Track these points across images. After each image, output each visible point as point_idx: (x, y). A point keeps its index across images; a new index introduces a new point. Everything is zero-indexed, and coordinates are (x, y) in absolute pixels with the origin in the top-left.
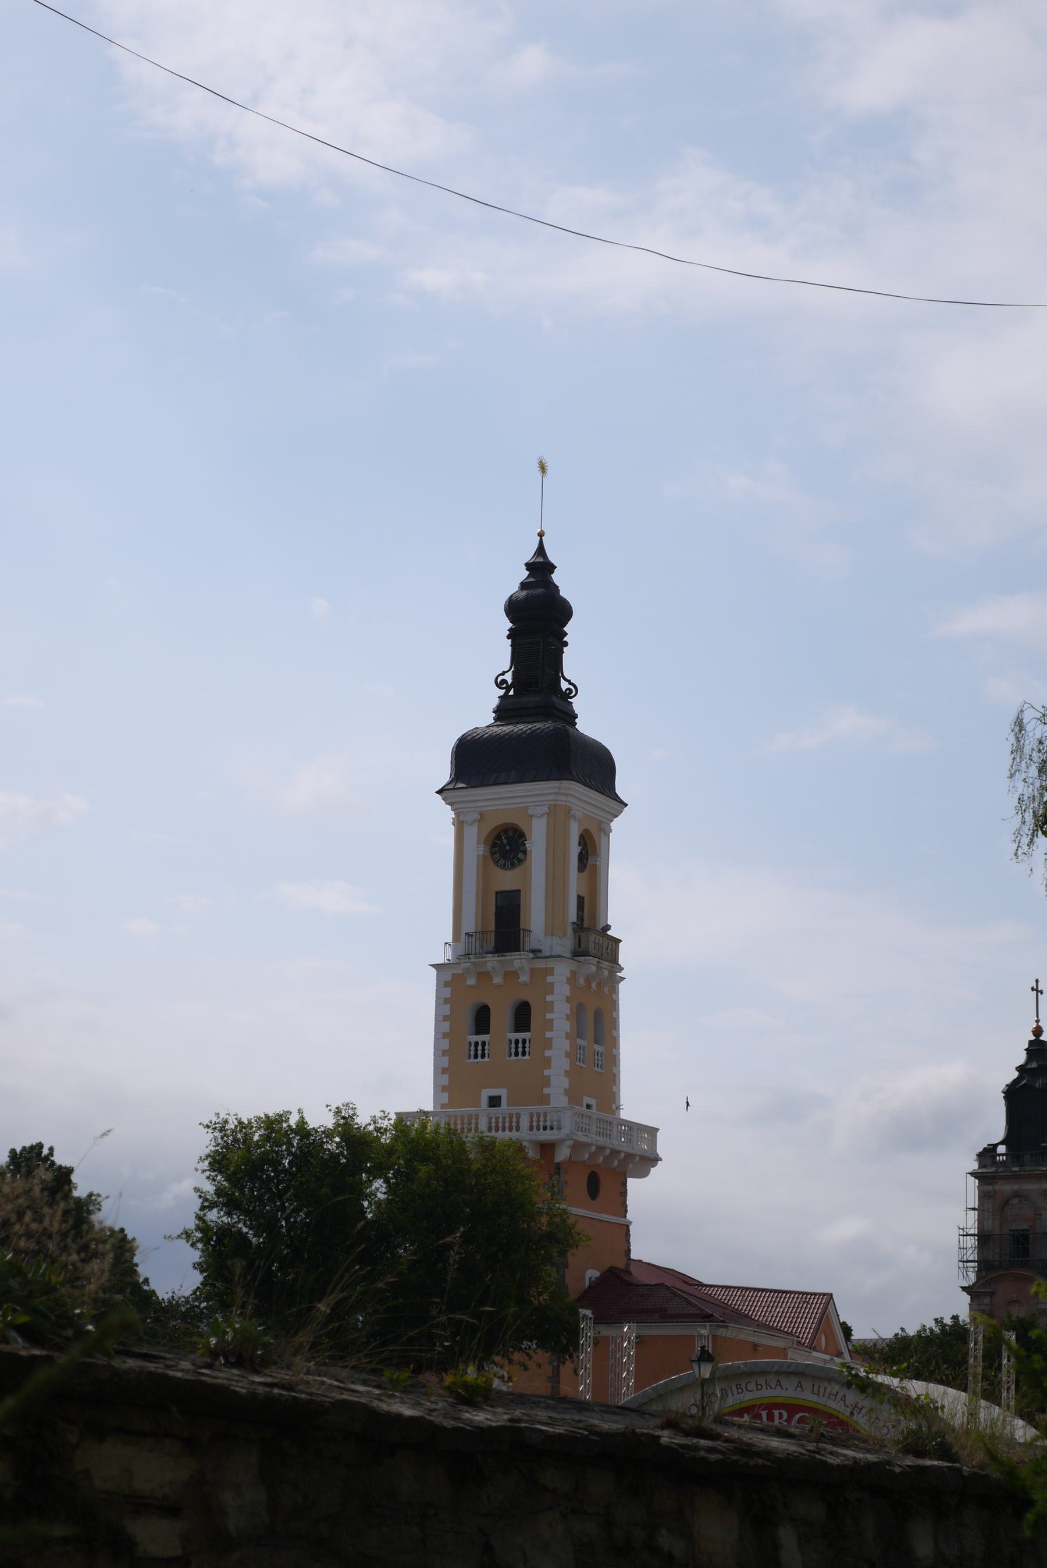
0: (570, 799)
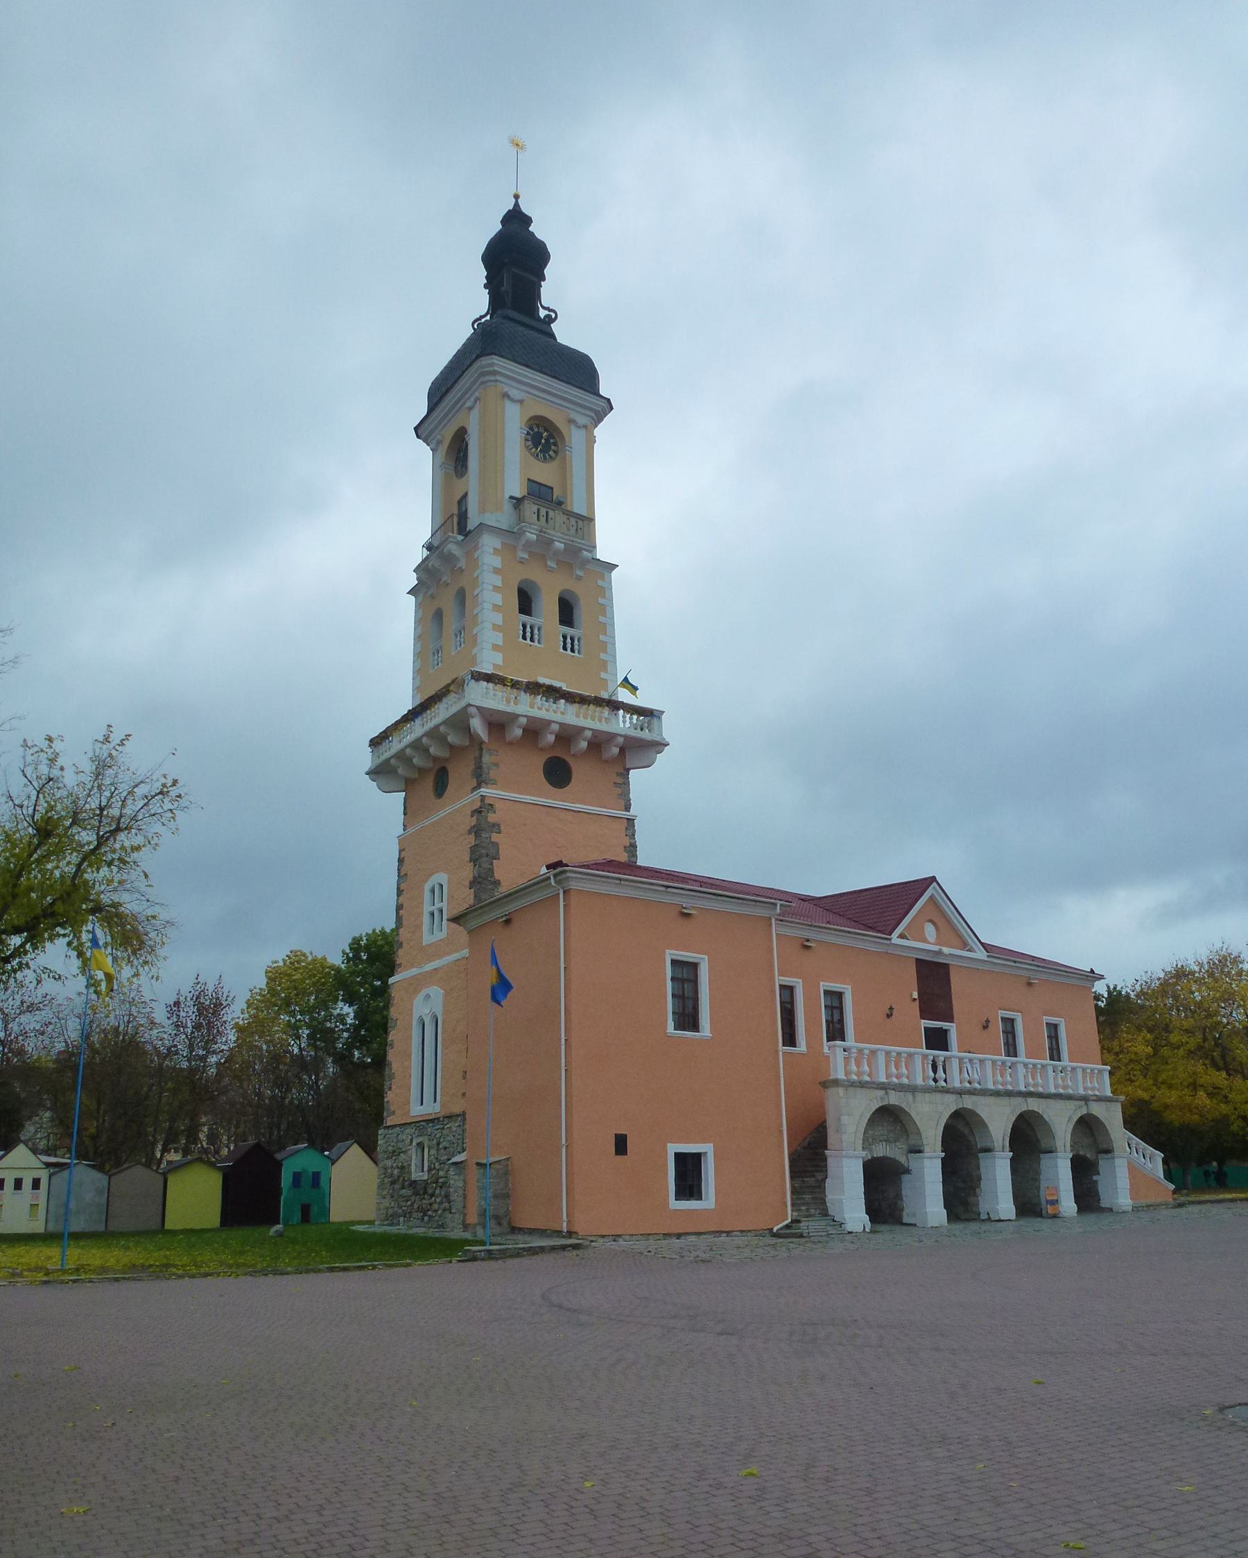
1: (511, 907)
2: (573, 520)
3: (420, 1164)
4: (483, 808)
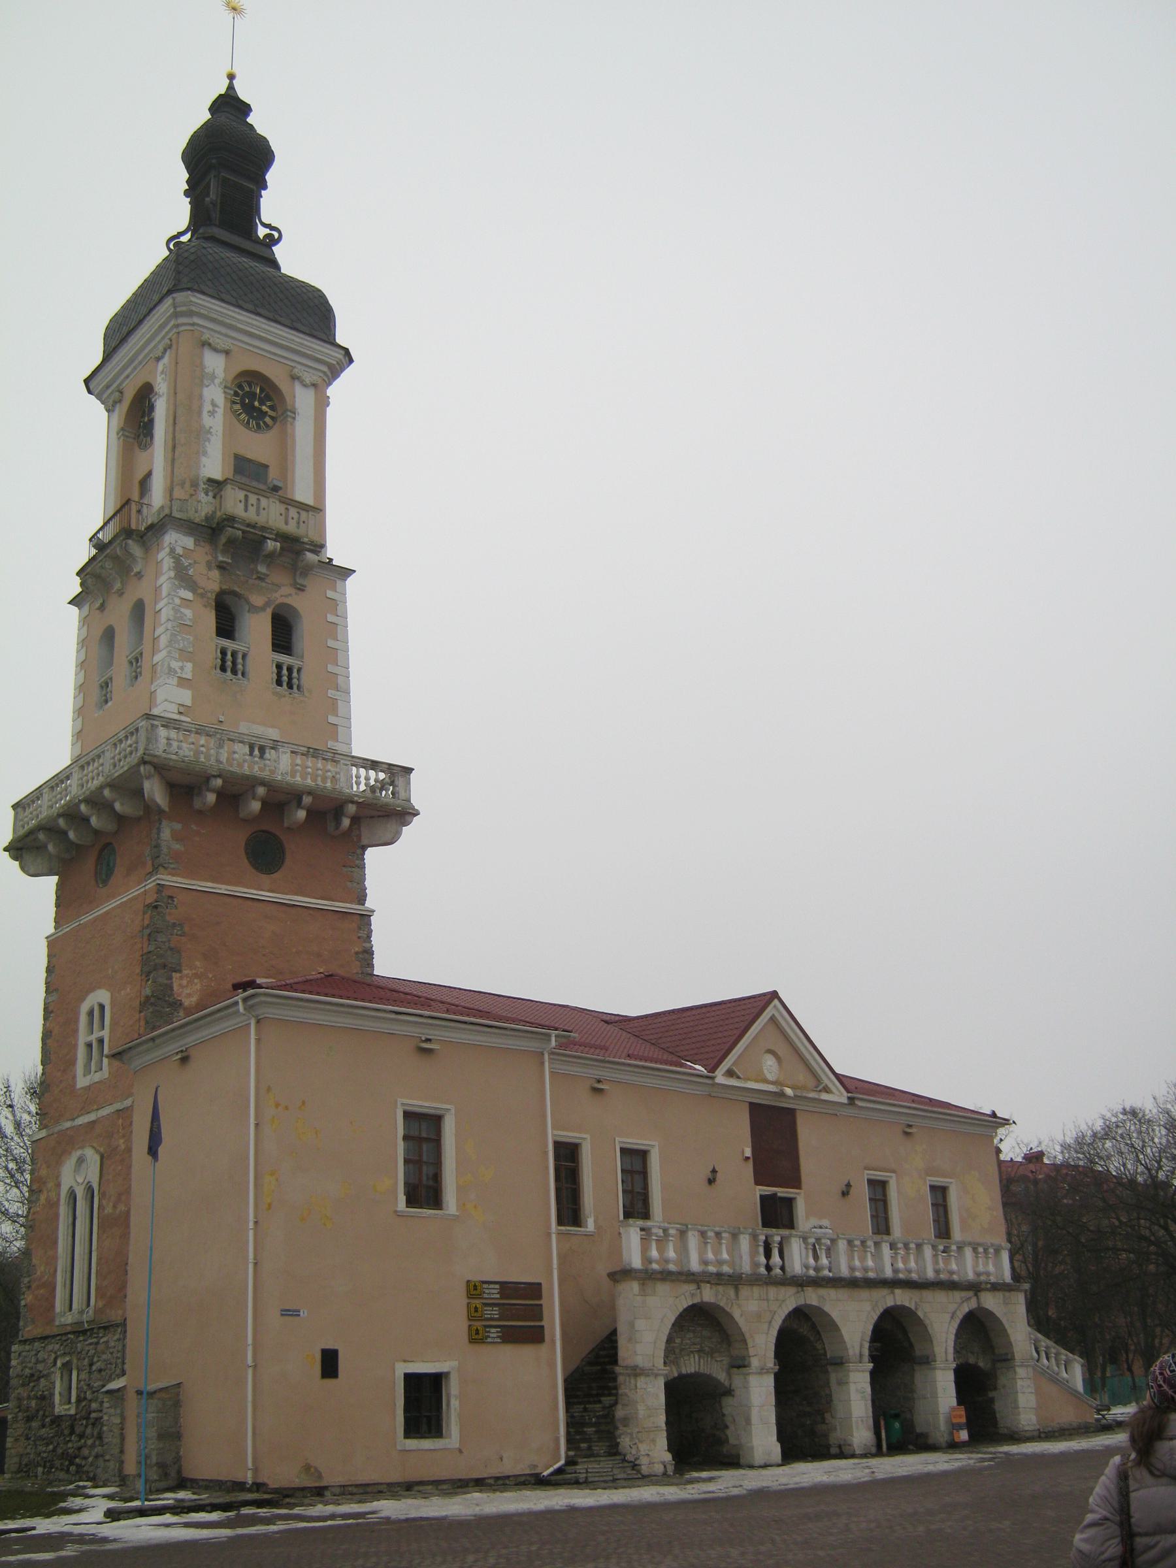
0: (196, 320)
1: (190, 1040)
2: (293, 512)
3: (66, 1393)
4: (162, 900)
